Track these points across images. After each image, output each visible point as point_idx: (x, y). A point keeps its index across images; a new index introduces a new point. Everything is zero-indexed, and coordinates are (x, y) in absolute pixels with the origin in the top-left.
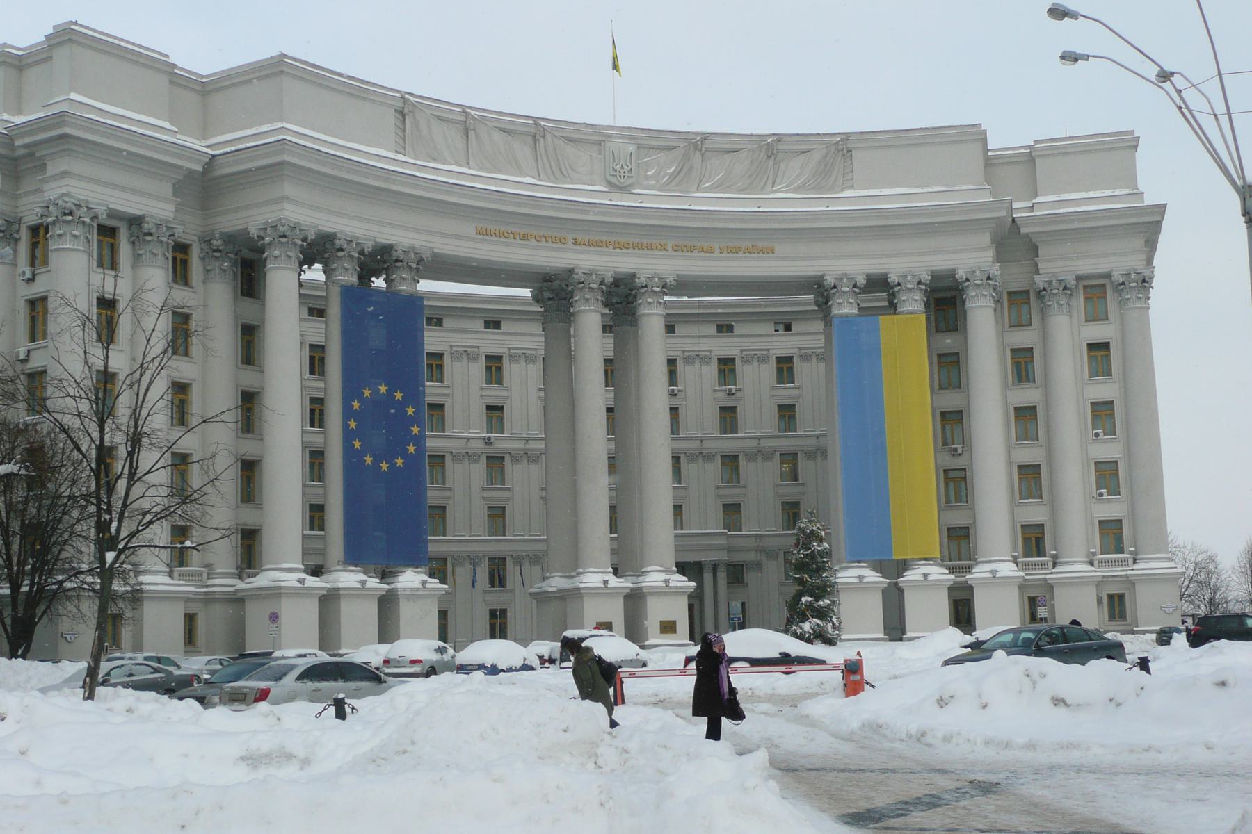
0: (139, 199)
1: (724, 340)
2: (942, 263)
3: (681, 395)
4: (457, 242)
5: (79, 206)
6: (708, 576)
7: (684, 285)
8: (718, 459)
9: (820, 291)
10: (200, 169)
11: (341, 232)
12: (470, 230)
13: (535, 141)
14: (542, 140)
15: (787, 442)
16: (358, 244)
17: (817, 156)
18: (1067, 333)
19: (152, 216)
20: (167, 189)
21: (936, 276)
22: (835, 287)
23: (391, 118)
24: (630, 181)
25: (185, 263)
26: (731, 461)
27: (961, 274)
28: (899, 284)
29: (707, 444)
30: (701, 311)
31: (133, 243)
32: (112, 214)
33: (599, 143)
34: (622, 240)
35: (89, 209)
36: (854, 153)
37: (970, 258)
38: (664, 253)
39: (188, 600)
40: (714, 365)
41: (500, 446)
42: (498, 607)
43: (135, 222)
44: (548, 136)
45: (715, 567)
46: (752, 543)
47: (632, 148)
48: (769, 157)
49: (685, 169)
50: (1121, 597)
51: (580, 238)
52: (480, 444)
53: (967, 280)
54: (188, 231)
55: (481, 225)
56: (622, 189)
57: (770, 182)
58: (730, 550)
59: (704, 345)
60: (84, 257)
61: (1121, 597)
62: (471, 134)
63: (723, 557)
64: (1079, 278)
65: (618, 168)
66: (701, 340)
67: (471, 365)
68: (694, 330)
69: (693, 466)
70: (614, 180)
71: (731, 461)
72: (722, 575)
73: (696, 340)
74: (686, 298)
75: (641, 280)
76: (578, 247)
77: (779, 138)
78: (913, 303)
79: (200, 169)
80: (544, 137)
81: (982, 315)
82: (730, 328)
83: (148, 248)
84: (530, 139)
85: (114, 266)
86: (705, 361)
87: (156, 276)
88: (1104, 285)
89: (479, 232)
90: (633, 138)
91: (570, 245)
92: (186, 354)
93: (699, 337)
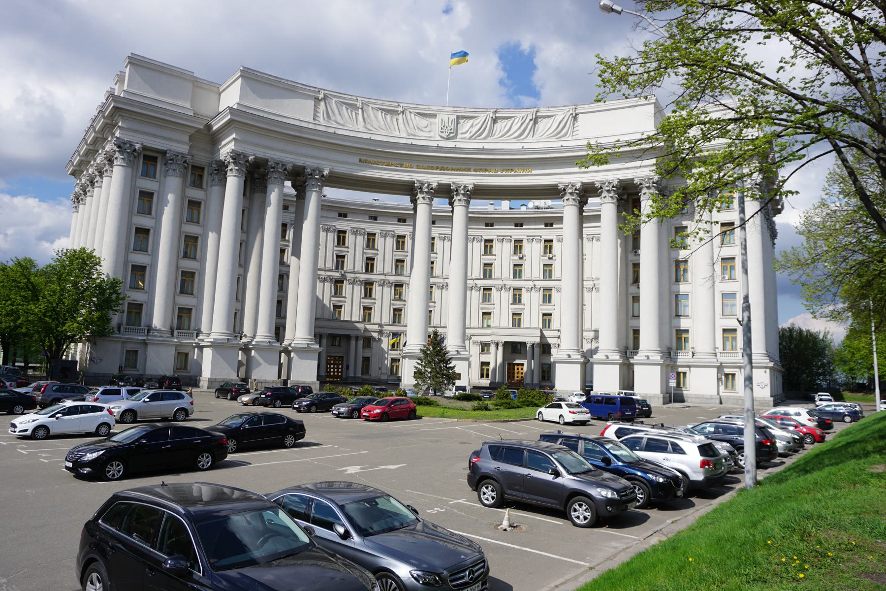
0: (165, 142)
2: (626, 175)
4: (347, 166)
5: (125, 143)
7: (480, 192)
10: (202, 127)
11: (272, 158)
12: (356, 160)
16: (283, 165)
20: (186, 138)
21: (620, 181)
22: (564, 190)
23: (311, 103)
25: (201, 177)
27: (637, 181)
28: (601, 188)
29: (535, 283)
31: (165, 164)
32: (144, 148)
34: (446, 166)
37: (643, 171)
39: (177, 346)
41: (432, 280)
43: (164, 153)
44: (408, 112)
46: (556, 333)
47: (453, 117)
50: (733, 375)
51: (421, 165)
53: (641, 184)
54: (201, 158)
55: (363, 158)
56: (448, 139)
57: (531, 133)
58: (542, 336)
60: (130, 170)
61: (733, 375)
79: (202, 127)
81: (647, 205)
82: (551, 225)
83: (171, 167)
85: (155, 177)
89: (360, 161)
90: (456, 112)
92: (198, 223)
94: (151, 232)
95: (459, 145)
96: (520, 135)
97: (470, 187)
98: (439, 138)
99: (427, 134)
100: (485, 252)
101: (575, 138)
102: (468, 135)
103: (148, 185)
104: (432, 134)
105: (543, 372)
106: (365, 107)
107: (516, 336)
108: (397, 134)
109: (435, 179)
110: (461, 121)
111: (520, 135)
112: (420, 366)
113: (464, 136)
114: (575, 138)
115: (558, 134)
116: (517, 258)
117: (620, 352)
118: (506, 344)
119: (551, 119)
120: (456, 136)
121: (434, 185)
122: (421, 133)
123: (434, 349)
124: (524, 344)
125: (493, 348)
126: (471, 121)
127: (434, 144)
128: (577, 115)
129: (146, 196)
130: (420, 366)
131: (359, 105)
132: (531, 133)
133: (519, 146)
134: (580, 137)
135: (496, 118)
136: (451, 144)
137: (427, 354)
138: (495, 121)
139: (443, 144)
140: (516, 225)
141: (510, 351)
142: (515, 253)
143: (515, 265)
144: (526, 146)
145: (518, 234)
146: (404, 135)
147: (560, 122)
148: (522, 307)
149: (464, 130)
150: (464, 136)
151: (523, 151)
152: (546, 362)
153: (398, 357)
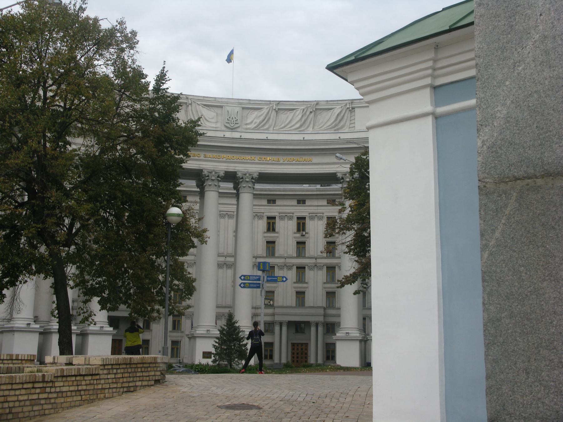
1: (301, 208)
3: (307, 235)
6: (313, 329)
8: (325, 268)
14: (190, 106)
17: (337, 111)
26: (301, 269)
29: (319, 261)
30: (318, 193)
33: (221, 107)
36: (356, 109)
38: (253, 161)
40: (325, 221)
44: (193, 104)
45: (317, 325)
47: (238, 109)
48: (311, 112)
49: (266, 120)
56: (232, 129)
57: (312, 125)
58: (325, 316)
59: (320, 210)
63: (321, 319)
65: (231, 119)
66: (319, 208)
67: (230, 220)
68: (315, 202)
69: (312, 273)
71: (301, 269)
72: (320, 329)
73: (316, 208)
74: (318, 186)
75: (239, 175)
76: (207, 159)
77: (318, 103)
80: (191, 104)
86: (320, 218)
90: (241, 104)
91: (202, 158)
93: (318, 206)
95: (245, 136)
97: (255, 175)
98: (224, 129)
99: (214, 125)
100: (269, 230)
101: (352, 130)
102: (252, 126)
104: (219, 125)
105: (328, 351)
107: (299, 315)
109: (222, 167)
110: (246, 112)
111: (301, 126)
112: (217, 345)
113: (248, 126)
114: (352, 130)
115: (336, 127)
116: (298, 235)
117: (360, 330)
118: (290, 324)
119: (330, 113)
121: (222, 174)
122: (208, 124)
123: (229, 329)
124: (308, 324)
125: (277, 328)
126: (256, 113)
127: (220, 134)
128: (353, 108)
130: (217, 345)
132: (312, 125)
133: (300, 137)
134: (357, 129)
135: (279, 109)
136: (236, 135)
137: (224, 334)
138: (278, 111)
139: (228, 134)
140: (299, 202)
141: (294, 331)
142: (299, 230)
143: (298, 243)
144: (308, 137)
145: (301, 211)
147: (338, 115)
148: (305, 285)
149: (249, 121)
150: (248, 126)
151: (304, 141)
152: (329, 341)
153: (179, 339)
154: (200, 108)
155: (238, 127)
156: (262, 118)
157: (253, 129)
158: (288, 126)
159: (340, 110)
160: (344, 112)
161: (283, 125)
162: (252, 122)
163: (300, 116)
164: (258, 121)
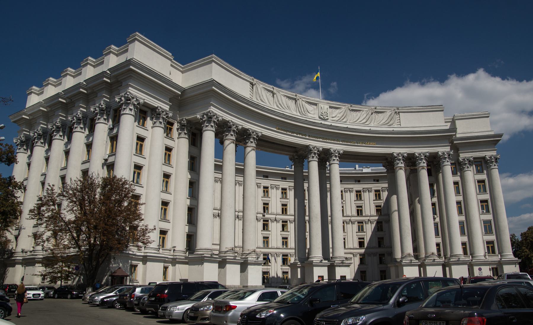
9: (389, 161)
13: (296, 101)
15: (360, 218)
17: (388, 113)
18: (471, 176)
19: (160, 107)
24: (327, 118)
35: (137, 100)
41: (267, 216)
42: (266, 270)
47: (328, 107)
51: (311, 135)
52: (261, 215)
62: (275, 96)
64: (474, 158)
70: (322, 117)
78: (423, 164)
79: (180, 93)
84: (294, 101)
87: (159, 132)
88: (481, 161)
90: (328, 103)
94: (144, 168)
96: (366, 122)
103: (142, 132)
106: (277, 93)
108: (295, 113)
111: (366, 122)
113: (334, 119)
120: (328, 119)
126: (338, 111)
129: (141, 139)
131: (275, 91)
132: (373, 121)
134: (402, 126)
146: (299, 115)
149: (334, 116)
150: (334, 119)
154: (304, 103)
155: (328, 119)
156: (342, 114)
157: (337, 121)
158: (359, 121)
159: (390, 113)
160: (393, 114)
161: (355, 120)
162: (335, 117)
163: (365, 115)
164: (340, 115)
